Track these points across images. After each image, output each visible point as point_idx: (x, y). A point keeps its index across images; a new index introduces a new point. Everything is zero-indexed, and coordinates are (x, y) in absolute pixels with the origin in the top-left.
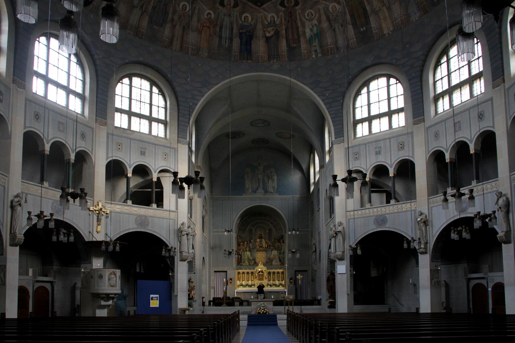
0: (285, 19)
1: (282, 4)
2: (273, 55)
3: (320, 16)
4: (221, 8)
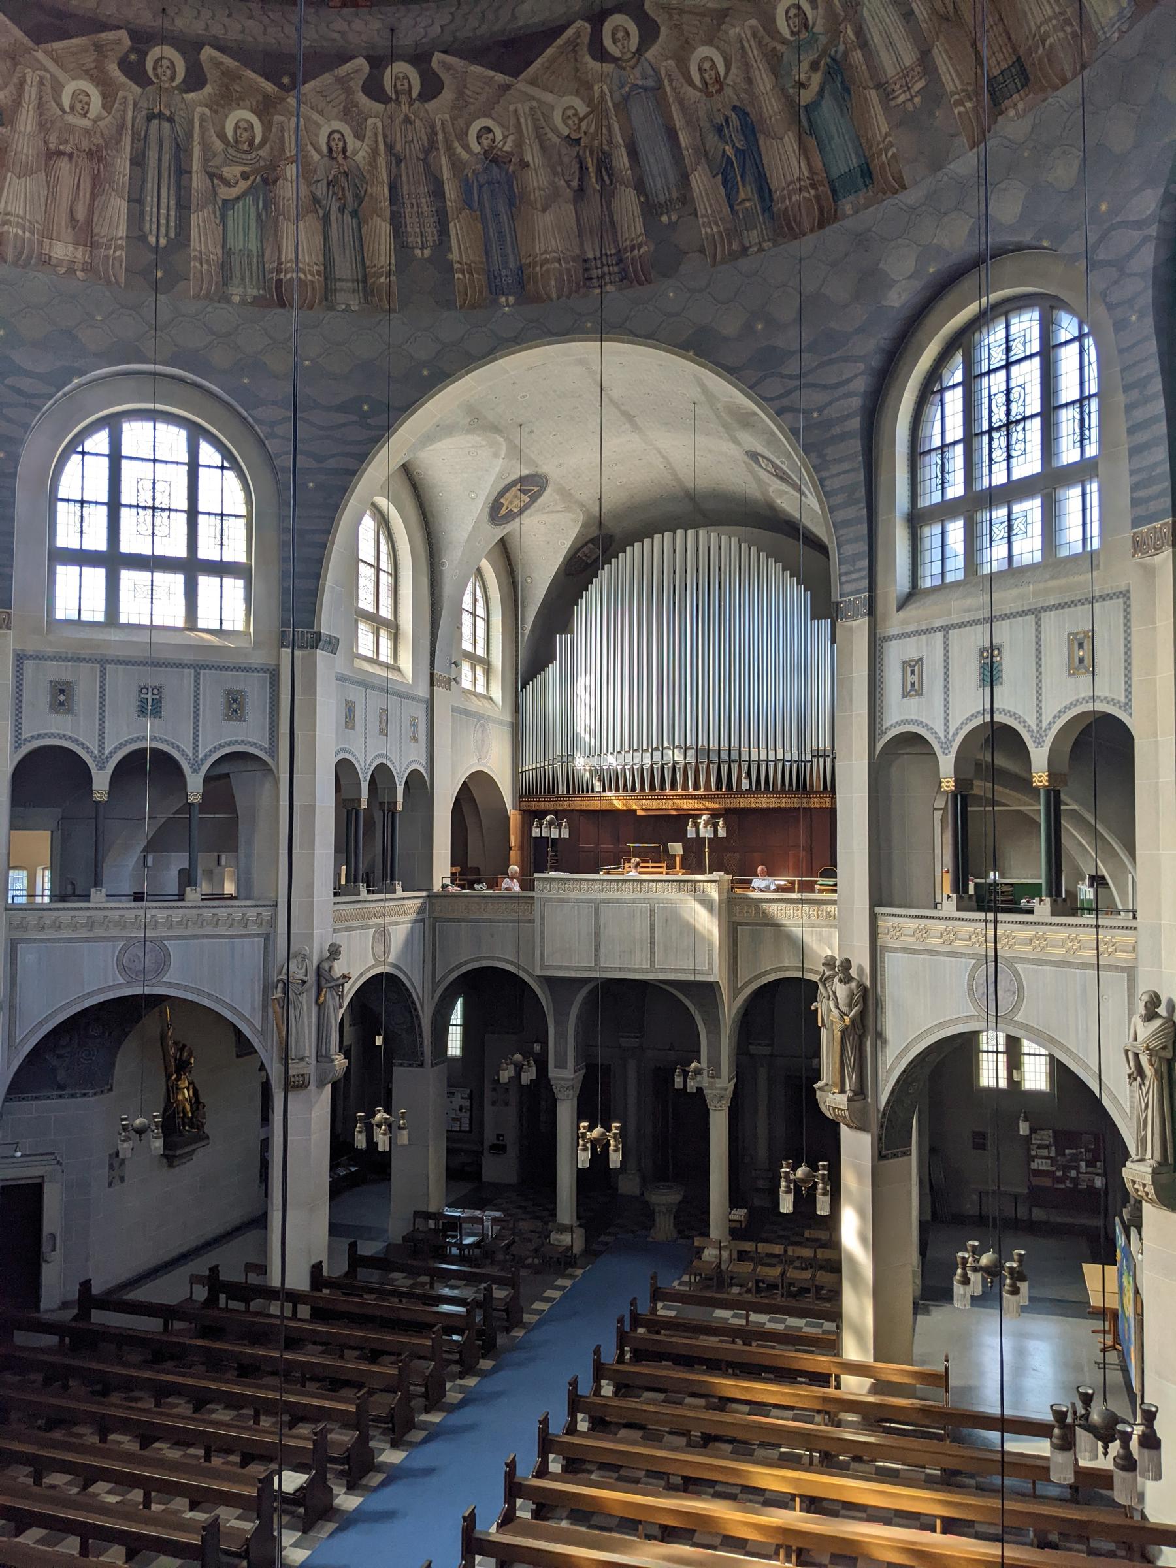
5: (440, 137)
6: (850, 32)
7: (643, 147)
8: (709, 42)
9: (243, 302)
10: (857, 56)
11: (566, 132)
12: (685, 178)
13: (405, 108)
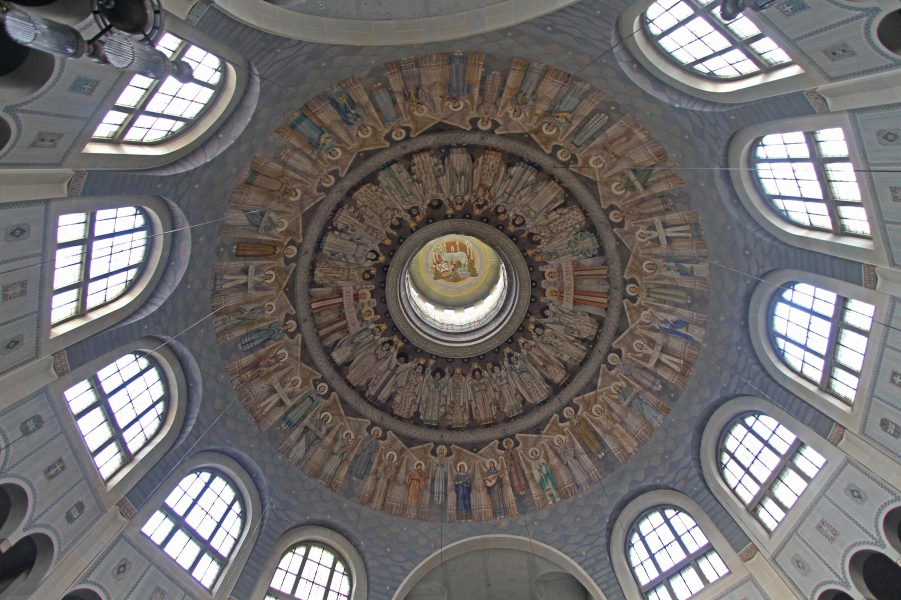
1: (501, 447)
3: (546, 452)
6: (313, 157)
7: (390, 104)
8: (365, 139)
9: (586, 83)
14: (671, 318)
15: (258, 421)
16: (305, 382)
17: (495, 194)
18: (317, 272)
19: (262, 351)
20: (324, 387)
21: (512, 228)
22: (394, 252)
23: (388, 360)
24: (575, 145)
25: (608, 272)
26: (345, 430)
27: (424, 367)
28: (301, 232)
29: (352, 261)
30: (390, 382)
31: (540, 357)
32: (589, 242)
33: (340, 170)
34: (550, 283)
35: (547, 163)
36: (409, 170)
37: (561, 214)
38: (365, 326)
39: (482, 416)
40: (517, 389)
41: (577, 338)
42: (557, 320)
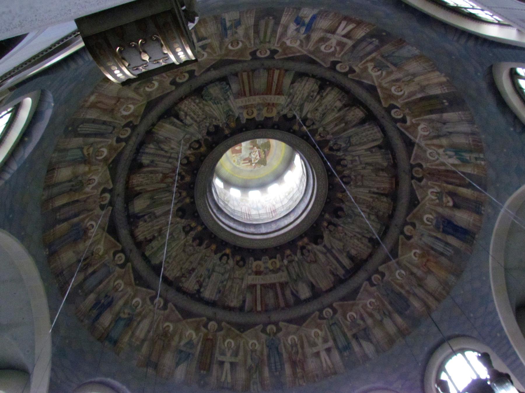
0: (436, 181)
1: (420, 180)
2: (476, 207)
3: (434, 145)
4: (412, 241)
5: (91, 213)
6: (138, 320)
8: (125, 284)
10: (135, 324)
11: (94, 250)
12: (91, 292)
13: (98, 200)
14: (293, 27)
15: (335, 373)
16: (318, 326)
17: (170, 169)
18: (232, 305)
19: (285, 356)
20: (327, 312)
21: (203, 149)
22: (222, 241)
23: (318, 253)
24: (114, 129)
25: (245, 71)
26: (366, 305)
27: (330, 223)
28: (198, 319)
29: (227, 276)
30: (337, 255)
31: (336, 125)
32: (214, 91)
33: (149, 296)
34: (259, 114)
35: (134, 141)
36: (150, 241)
37: (186, 114)
38: (284, 268)
39: (385, 185)
40: (366, 150)
41: (318, 93)
42: (298, 108)
